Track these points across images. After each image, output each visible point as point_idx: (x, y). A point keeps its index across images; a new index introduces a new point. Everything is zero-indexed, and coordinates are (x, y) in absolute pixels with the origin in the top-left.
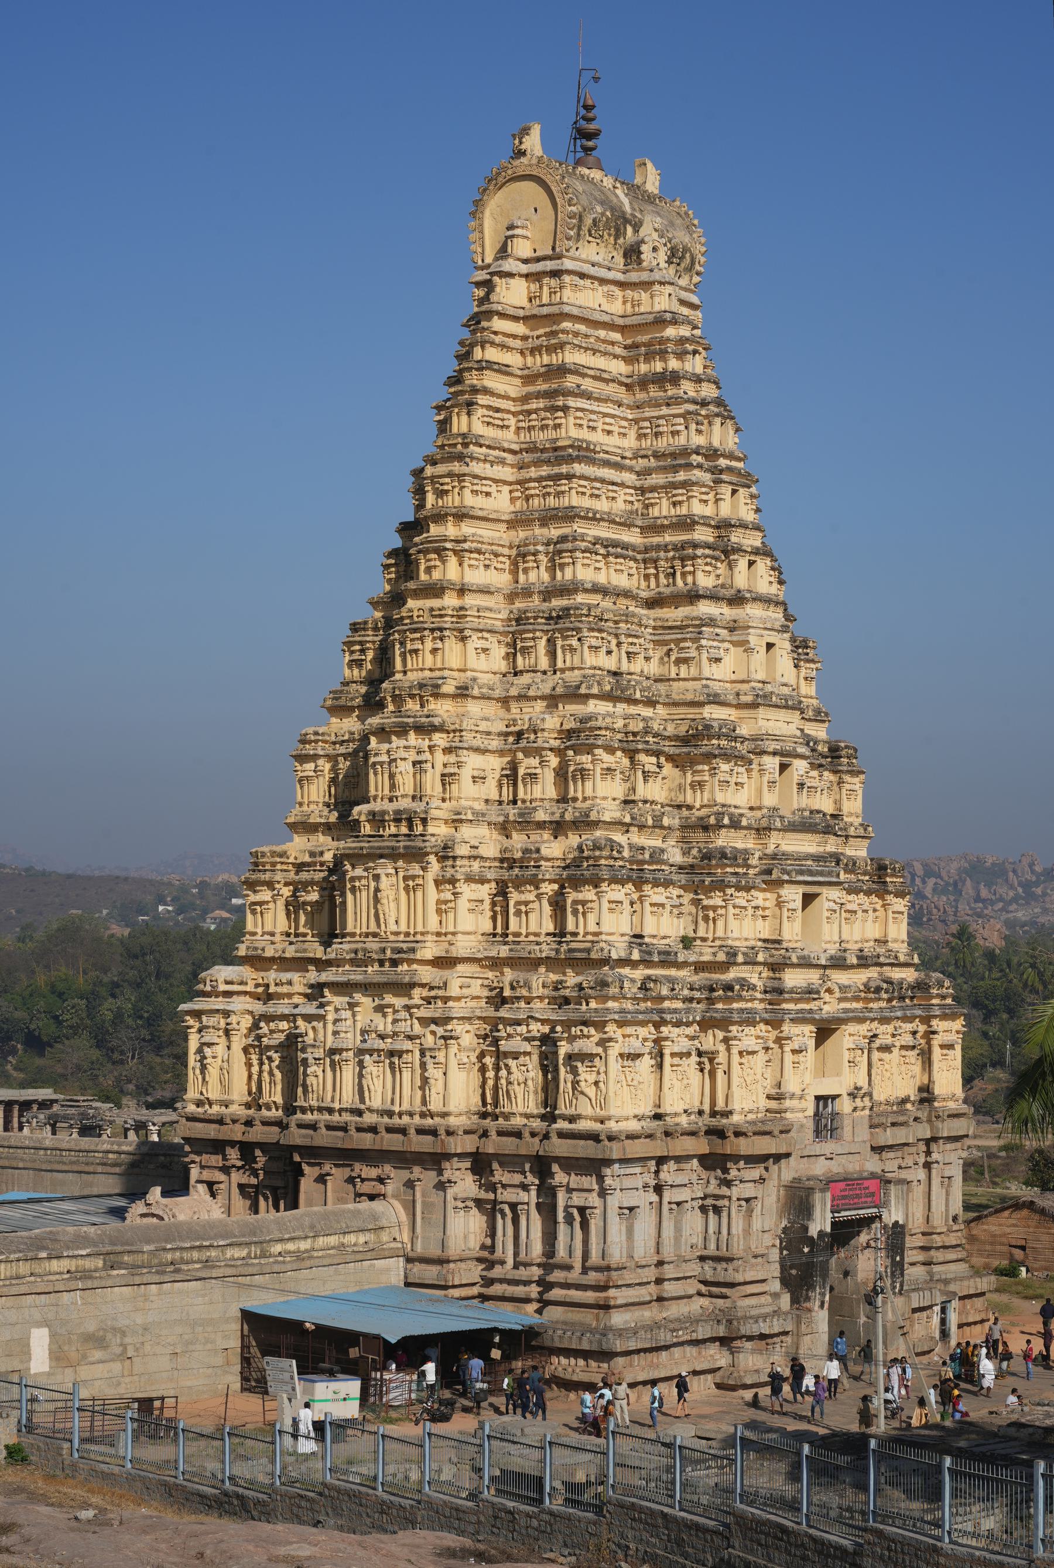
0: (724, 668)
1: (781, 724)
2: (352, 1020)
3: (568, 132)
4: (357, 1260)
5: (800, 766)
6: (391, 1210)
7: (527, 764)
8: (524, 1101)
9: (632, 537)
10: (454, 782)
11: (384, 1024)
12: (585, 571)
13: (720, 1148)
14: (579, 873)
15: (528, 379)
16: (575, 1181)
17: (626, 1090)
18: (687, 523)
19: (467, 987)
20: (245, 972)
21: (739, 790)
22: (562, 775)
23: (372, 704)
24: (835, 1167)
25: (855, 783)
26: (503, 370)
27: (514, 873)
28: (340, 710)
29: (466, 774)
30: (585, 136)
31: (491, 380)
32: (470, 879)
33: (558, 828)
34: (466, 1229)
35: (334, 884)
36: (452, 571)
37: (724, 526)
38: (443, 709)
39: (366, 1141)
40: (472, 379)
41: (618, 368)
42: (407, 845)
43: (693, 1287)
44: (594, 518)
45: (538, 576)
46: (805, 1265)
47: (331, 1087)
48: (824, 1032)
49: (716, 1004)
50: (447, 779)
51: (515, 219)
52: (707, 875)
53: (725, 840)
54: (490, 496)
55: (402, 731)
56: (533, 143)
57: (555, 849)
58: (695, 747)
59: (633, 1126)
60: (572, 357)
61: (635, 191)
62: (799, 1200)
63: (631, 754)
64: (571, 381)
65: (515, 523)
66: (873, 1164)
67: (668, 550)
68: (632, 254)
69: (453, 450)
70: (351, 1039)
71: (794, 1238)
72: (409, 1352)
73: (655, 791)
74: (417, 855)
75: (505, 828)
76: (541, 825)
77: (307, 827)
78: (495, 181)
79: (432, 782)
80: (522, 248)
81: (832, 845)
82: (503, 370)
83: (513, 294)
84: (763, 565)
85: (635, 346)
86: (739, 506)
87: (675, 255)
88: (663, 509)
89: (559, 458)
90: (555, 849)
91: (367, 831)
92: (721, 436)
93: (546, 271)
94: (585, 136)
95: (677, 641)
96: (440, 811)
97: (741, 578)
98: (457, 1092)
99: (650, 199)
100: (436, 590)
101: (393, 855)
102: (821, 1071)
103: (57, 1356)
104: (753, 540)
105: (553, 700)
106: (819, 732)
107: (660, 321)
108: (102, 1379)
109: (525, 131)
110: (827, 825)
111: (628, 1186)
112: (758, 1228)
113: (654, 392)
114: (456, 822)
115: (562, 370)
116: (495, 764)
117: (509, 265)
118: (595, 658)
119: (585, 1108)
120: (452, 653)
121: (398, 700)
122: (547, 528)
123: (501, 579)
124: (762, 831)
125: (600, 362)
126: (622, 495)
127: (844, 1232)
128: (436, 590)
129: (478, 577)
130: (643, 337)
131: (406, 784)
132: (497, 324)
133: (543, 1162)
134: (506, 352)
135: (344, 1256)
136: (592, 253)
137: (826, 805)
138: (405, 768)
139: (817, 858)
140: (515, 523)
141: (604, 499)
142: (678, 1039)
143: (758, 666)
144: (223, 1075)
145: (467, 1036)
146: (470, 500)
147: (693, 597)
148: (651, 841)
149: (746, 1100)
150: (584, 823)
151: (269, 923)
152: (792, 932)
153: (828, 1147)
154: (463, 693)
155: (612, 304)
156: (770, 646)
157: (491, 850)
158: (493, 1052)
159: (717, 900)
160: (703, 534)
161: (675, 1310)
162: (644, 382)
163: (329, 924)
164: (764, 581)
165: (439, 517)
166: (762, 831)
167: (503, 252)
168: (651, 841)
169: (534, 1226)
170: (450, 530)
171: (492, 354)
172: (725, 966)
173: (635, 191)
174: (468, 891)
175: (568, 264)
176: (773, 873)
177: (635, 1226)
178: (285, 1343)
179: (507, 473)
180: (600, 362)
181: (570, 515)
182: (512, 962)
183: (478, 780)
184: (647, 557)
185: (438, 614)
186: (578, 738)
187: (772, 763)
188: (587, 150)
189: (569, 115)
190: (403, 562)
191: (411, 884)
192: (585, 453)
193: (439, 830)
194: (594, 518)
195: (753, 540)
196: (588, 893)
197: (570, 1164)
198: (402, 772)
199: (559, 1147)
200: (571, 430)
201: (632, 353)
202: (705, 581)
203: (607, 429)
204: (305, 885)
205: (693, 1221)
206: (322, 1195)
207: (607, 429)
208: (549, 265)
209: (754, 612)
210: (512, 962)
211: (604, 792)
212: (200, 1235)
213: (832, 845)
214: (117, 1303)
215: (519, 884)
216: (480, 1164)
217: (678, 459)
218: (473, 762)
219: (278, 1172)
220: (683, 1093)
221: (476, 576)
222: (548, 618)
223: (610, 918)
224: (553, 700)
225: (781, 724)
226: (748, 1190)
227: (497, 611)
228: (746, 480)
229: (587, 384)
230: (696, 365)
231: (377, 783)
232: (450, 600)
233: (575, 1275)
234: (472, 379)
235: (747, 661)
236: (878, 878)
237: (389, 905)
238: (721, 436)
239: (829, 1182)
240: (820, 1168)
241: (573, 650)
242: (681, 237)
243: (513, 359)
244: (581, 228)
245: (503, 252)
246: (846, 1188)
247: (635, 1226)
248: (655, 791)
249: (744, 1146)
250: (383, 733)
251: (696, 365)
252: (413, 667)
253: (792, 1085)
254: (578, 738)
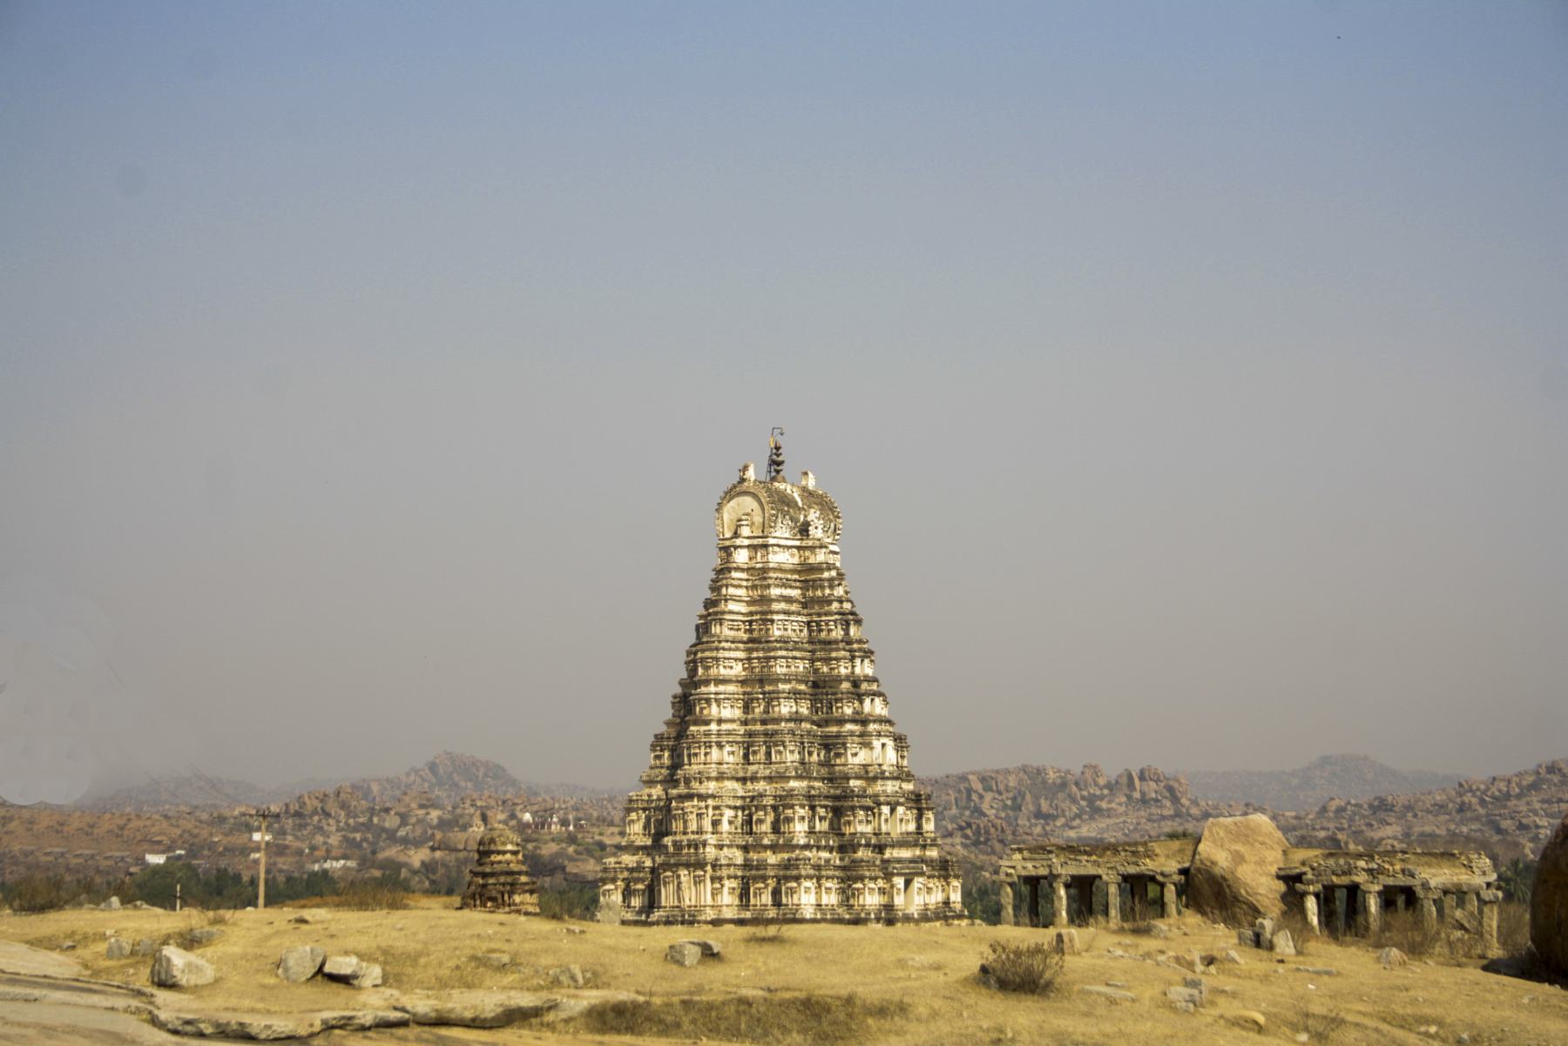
3: (766, 461)
5: (900, 810)
23: (671, 781)
28: (650, 783)
31: (732, 606)
32: (729, 877)
33: (774, 848)
55: (690, 797)
74: (700, 865)
75: (745, 849)
76: (766, 847)
77: (632, 849)
83: (741, 557)
84: (878, 700)
85: (806, 581)
90: (772, 858)
101: (687, 866)
109: (745, 468)
114: (720, 847)
117: (738, 542)
121: (687, 781)
129: (724, 711)
131: (693, 826)
132: (735, 574)
146: (722, 671)
156: (883, 745)
165: (707, 682)
167: (736, 535)
171: (731, 591)
174: (728, 884)
175: (771, 541)
179: (741, 655)
185: (708, 734)
187: (886, 809)
188: (778, 472)
191: (698, 881)
202: (848, 711)
204: (637, 880)
208: (760, 541)
215: (756, 879)
221: (727, 713)
228: (868, 654)
231: (677, 826)
232: (713, 727)
241: (780, 752)
243: (742, 592)
245: (736, 535)
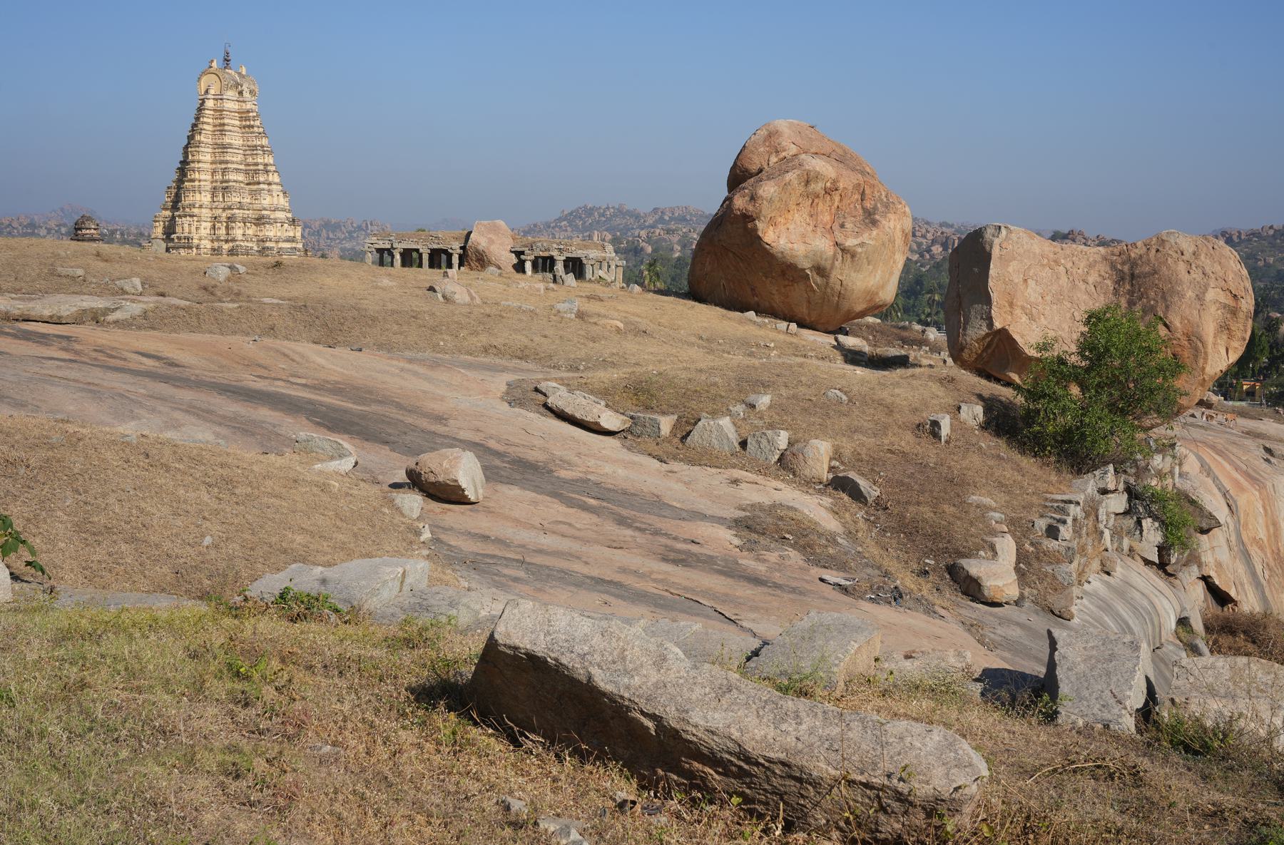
0: (266, 201)
1: (281, 215)
7: (218, 225)
9: (242, 167)
12: (232, 176)
18: (257, 164)
21: (270, 232)
22: (227, 228)
30: (227, 60)
31: (205, 127)
33: (227, 241)
36: (197, 176)
37: (266, 165)
38: (196, 211)
41: (237, 123)
44: (233, 163)
45: (219, 177)
50: (197, 229)
53: (268, 244)
56: (214, 64)
57: (226, 247)
58: (260, 221)
60: (226, 121)
61: (240, 74)
65: (212, 163)
67: (252, 172)
68: (241, 93)
73: (250, 232)
75: (212, 241)
78: (204, 73)
79: (193, 229)
80: (212, 92)
81: (294, 245)
83: (210, 104)
88: (250, 160)
89: (224, 147)
90: (226, 247)
92: (265, 142)
94: (227, 60)
95: (255, 194)
96: (196, 237)
97: (271, 179)
100: (193, 181)
104: (273, 168)
105: (224, 209)
106: (290, 215)
107: (248, 112)
110: (292, 240)
114: (200, 239)
115: (224, 125)
116: (209, 225)
118: (235, 199)
122: (221, 165)
123: (209, 177)
124: (277, 242)
128: (193, 181)
129: (203, 176)
131: (186, 229)
136: (231, 94)
137: (291, 234)
138: (186, 226)
140: (212, 163)
141: (235, 157)
147: (259, 183)
148: (250, 245)
150: (233, 240)
154: (201, 207)
157: (209, 246)
160: (261, 167)
164: (276, 178)
166: (277, 242)
167: (207, 92)
168: (250, 245)
170: (197, 165)
173: (240, 74)
181: (227, 162)
184: (246, 172)
186: (231, 219)
189: (222, 55)
192: (230, 146)
193: (196, 241)
194: (233, 163)
195: (273, 168)
200: (227, 140)
201: (241, 119)
202: (262, 179)
209: (274, 187)
211: (238, 232)
213: (294, 245)
217: (255, 147)
218: (204, 224)
221: (203, 177)
224: (224, 209)
225: (281, 215)
227: (208, 186)
230: (257, 123)
231: (178, 229)
238: (265, 142)
242: (252, 87)
243: (210, 121)
244: (228, 88)
245: (207, 92)
248: (250, 232)
250: (180, 216)
251: (257, 123)
252: (187, 200)
254: (231, 219)
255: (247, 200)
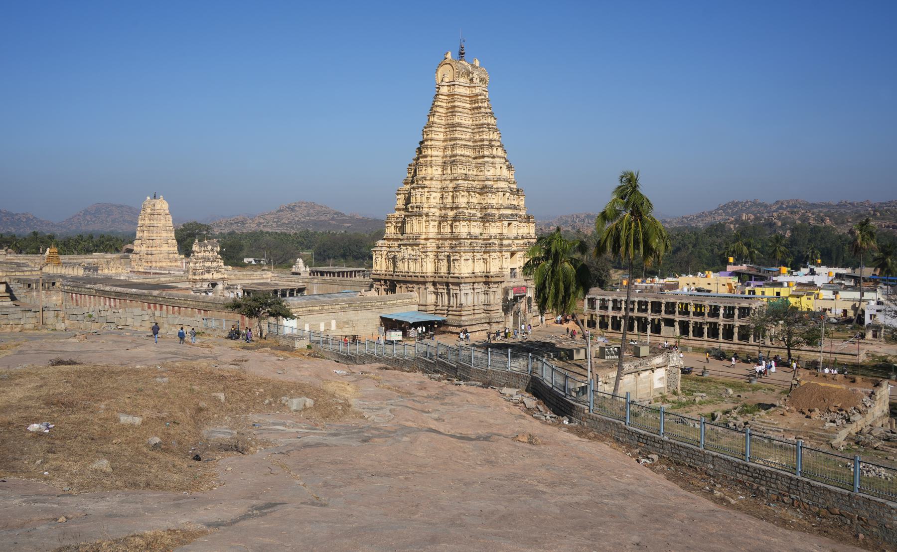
0: (490, 172)
1: (504, 185)
2: (408, 252)
4: (407, 306)
5: (508, 194)
6: (415, 294)
7: (445, 195)
8: (443, 270)
9: (471, 144)
10: (429, 200)
11: (413, 253)
12: (459, 151)
13: (487, 280)
14: (456, 219)
15: (448, 109)
16: (454, 287)
17: (465, 267)
18: (482, 140)
19: (431, 245)
20: (385, 242)
21: (493, 200)
22: (453, 197)
23: (413, 182)
24: (515, 284)
25: (523, 198)
26: (442, 107)
27: (443, 219)
28: (406, 183)
29: (432, 197)
30: (462, 54)
31: (439, 109)
33: (452, 209)
34: (431, 298)
35: (404, 222)
36: (429, 152)
37: (491, 141)
38: (427, 183)
39: (410, 279)
40: (435, 109)
41: (468, 106)
42: (419, 214)
43: (481, 311)
45: (449, 153)
46: (508, 306)
47: (403, 267)
48: (513, 254)
49: (487, 248)
51: (445, 73)
52: (485, 219)
53: (489, 211)
54: (438, 135)
55: (418, 188)
56: (449, 56)
57: (451, 214)
58: (483, 191)
59: (467, 275)
60: (456, 104)
61: (473, 66)
62: (506, 292)
63: (469, 192)
64: (457, 109)
65: (443, 141)
66: (525, 284)
67: (478, 146)
68: (471, 80)
69: (430, 125)
70: (407, 257)
71: (505, 300)
72: (416, 325)
74: (421, 215)
75: (440, 209)
77: (399, 210)
78: (441, 65)
80: (446, 80)
81: (516, 212)
82: (442, 107)
83: (444, 90)
84: (500, 149)
86: (495, 136)
87: (481, 80)
88: (477, 137)
89: (453, 127)
90: (451, 214)
91: (412, 211)
92: (491, 120)
93: (451, 85)
94: (462, 54)
95: (479, 166)
96: (426, 205)
97: (495, 152)
98: (429, 268)
99: (476, 68)
100: (426, 156)
101: (416, 216)
102: (512, 263)
103: (338, 326)
105: (451, 180)
106: (514, 187)
107: (477, 95)
108: (348, 331)
110: (515, 207)
111: (466, 289)
112: (496, 298)
113: (476, 111)
116: (439, 195)
117: (443, 83)
118: (460, 171)
119: (456, 271)
120: (429, 170)
122: (451, 142)
123: (441, 154)
124: (499, 209)
125: (464, 105)
126: (468, 134)
127: (516, 299)
128: (426, 156)
129: (435, 153)
130: (474, 98)
131: (419, 200)
132: (440, 97)
133: (447, 283)
134: (443, 104)
135: (404, 304)
136: (463, 80)
137: (516, 203)
138: (419, 196)
139: (512, 215)
140: (443, 141)
141: (464, 135)
142: (478, 256)
143: (498, 172)
144: (381, 265)
145: (431, 255)
146: (434, 136)
147: (483, 157)
149: (494, 269)
150: (457, 208)
151: (390, 231)
152: (505, 231)
153: (514, 280)
154: (431, 179)
155: (467, 92)
157: (437, 214)
158: (437, 259)
159: (487, 224)
160: (486, 143)
161: (477, 316)
162: (474, 109)
163: (402, 230)
164: (500, 152)
165: (427, 140)
166: (499, 209)
169: (446, 297)
170: (429, 143)
171: (439, 103)
172: (489, 239)
173: (473, 66)
174: (432, 223)
176: (501, 219)
177: (468, 297)
178: (389, 324)
179: (443, 130)
180: (464, 105)
181: (456, 139)
182: (441, 239)
183: (435, 198)
186: (456, 189)
190: (420, 150)
191: (419, 222)
192: (459, 125)
193: (426, 210)
195: (498, 144)
196: (458, 223)
197: (453, 284)
198: (418, 197)
199: (451, 280)
200: (456, 120)
201: (471, 102)
202: (486, 153)
203: (465, 119)
205: (482, 297)
206: (401, 290)
207: (465, 119)
209: (497, 160)
210: (441, 239)
211: (462, 201)
212: (371, 300)
213: (516, 212)
214: (351, 315)
215: (443, 221)
216: (434, 284)
217: (481, 126)
218: (433, 195)
219: (392, 285)
220: (479, 268)
222: (451, 162)
223: (463, 229)
224: (451, 180)
225: (504, 185)
226: (494, 289)
227: (440, 161)
228: (496, 130)
229: (460, 110)
230: (485, 105)
231: (413, 200)
232: (429, 159)
233: (454, 309)
234: (435, 109)
235: (496, 171)
236: (528, 219)
237: (415, 227)
238: (491, 120)
239: (513, 288)
240: (512, 284)
242: (483, 76)
243: (444, 105)
245: (442, 81)
246: (518, 289)
247: (468, 297)
249: (493, 280)
250: (414, 188)
251: (485, 105)
252: (420, 174)
253: (505, 266)
254: (456, 189)
255: (473, 172)
